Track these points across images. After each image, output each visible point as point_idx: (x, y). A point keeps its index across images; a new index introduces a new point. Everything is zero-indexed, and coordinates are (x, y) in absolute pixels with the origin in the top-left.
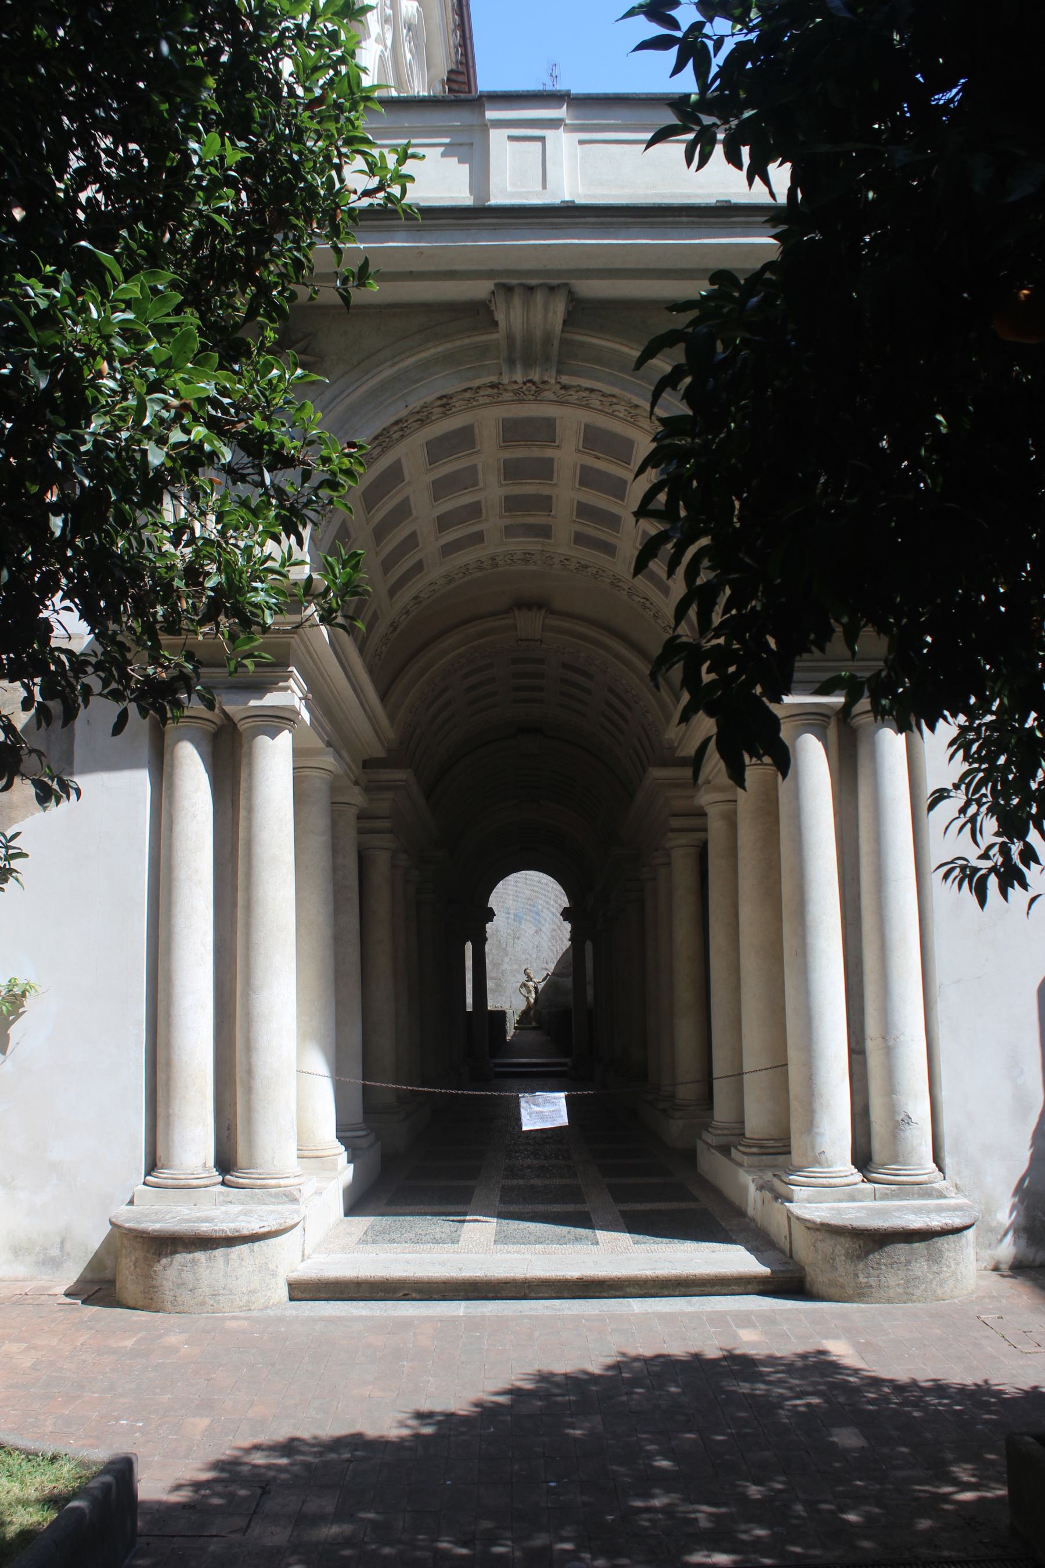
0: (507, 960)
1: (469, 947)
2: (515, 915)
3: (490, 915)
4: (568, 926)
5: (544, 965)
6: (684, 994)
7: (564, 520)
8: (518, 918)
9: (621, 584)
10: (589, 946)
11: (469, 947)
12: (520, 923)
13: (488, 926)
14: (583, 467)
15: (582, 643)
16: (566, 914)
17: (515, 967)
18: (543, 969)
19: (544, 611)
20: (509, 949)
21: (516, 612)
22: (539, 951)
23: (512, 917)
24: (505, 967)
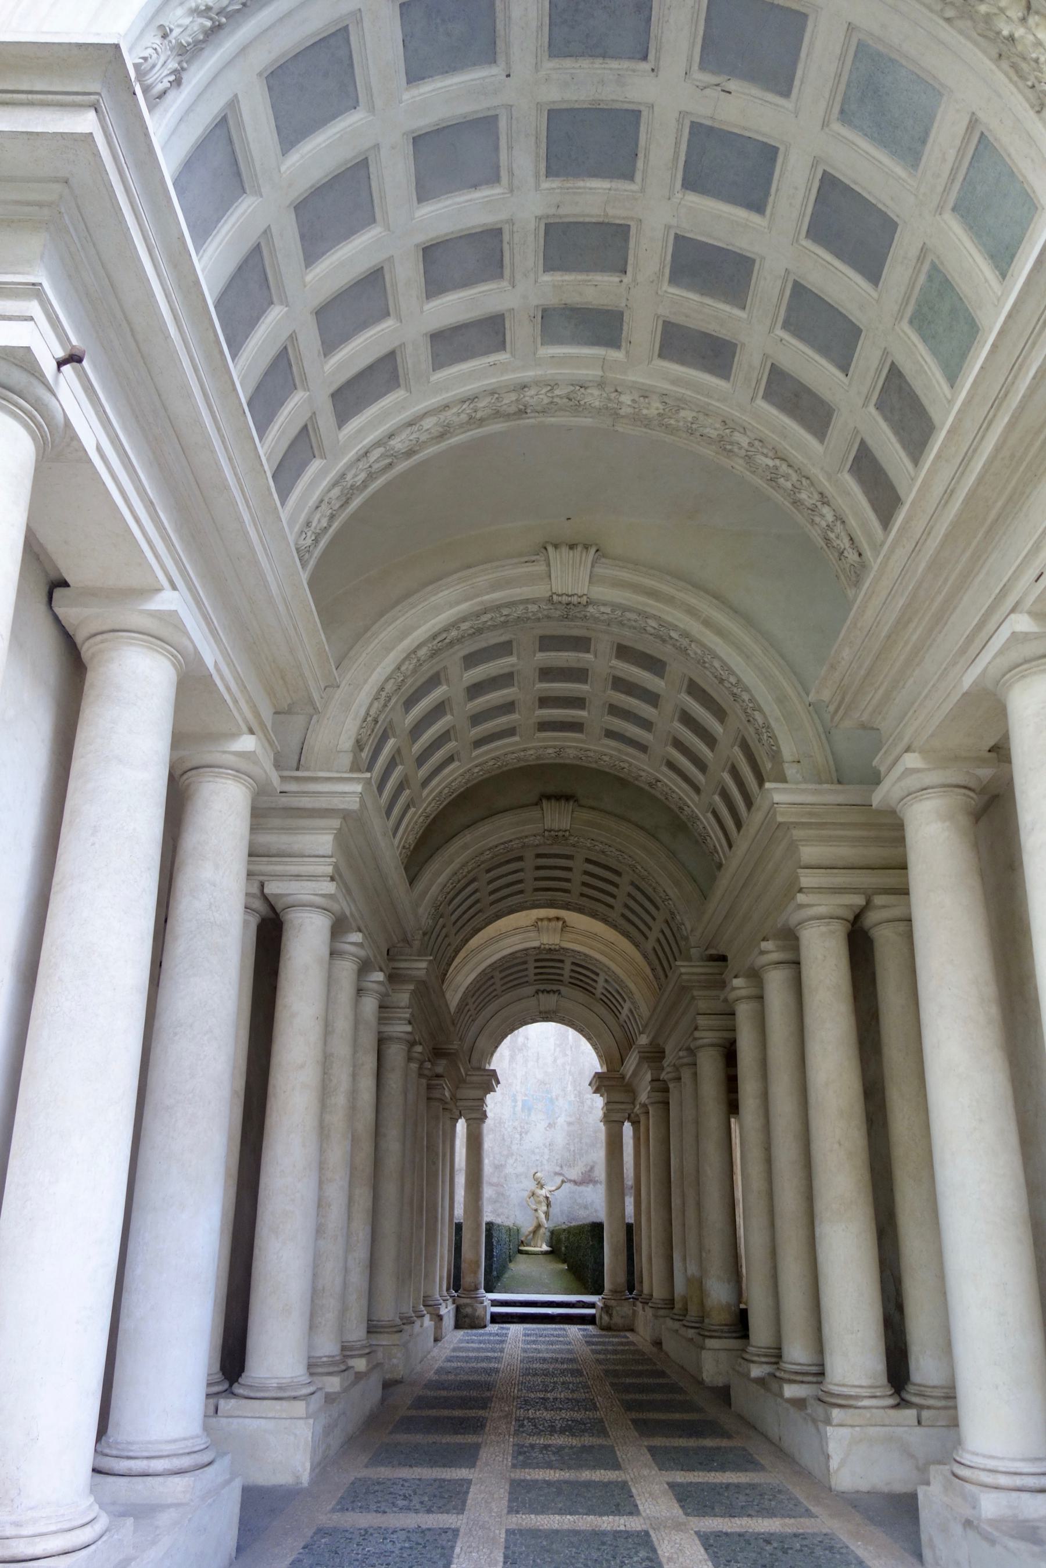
0: (511, 1161)
1: (461, 1126)
2: (524, 1102)
3: (489, 1081)
4: (598, 1102)
5: (558, 1169)
6: (841, 1180)
7: (647, 293)
8: (527, 1108)
9: (737, 437)
10: (628, 1128)
11: (461, 1126)
12: (529, 1115)
13: (490, 1098)
14: (696, 128)
15: (651, 602)
16: (601, 1083)
17: (520, 1169)
18: (556, 1174)
19: (593, 551)
20: (514, 1147)
21: (550, 549)
22: (551, 1151)
23: (520, 1104)
24: (509, 1170)
